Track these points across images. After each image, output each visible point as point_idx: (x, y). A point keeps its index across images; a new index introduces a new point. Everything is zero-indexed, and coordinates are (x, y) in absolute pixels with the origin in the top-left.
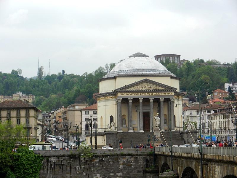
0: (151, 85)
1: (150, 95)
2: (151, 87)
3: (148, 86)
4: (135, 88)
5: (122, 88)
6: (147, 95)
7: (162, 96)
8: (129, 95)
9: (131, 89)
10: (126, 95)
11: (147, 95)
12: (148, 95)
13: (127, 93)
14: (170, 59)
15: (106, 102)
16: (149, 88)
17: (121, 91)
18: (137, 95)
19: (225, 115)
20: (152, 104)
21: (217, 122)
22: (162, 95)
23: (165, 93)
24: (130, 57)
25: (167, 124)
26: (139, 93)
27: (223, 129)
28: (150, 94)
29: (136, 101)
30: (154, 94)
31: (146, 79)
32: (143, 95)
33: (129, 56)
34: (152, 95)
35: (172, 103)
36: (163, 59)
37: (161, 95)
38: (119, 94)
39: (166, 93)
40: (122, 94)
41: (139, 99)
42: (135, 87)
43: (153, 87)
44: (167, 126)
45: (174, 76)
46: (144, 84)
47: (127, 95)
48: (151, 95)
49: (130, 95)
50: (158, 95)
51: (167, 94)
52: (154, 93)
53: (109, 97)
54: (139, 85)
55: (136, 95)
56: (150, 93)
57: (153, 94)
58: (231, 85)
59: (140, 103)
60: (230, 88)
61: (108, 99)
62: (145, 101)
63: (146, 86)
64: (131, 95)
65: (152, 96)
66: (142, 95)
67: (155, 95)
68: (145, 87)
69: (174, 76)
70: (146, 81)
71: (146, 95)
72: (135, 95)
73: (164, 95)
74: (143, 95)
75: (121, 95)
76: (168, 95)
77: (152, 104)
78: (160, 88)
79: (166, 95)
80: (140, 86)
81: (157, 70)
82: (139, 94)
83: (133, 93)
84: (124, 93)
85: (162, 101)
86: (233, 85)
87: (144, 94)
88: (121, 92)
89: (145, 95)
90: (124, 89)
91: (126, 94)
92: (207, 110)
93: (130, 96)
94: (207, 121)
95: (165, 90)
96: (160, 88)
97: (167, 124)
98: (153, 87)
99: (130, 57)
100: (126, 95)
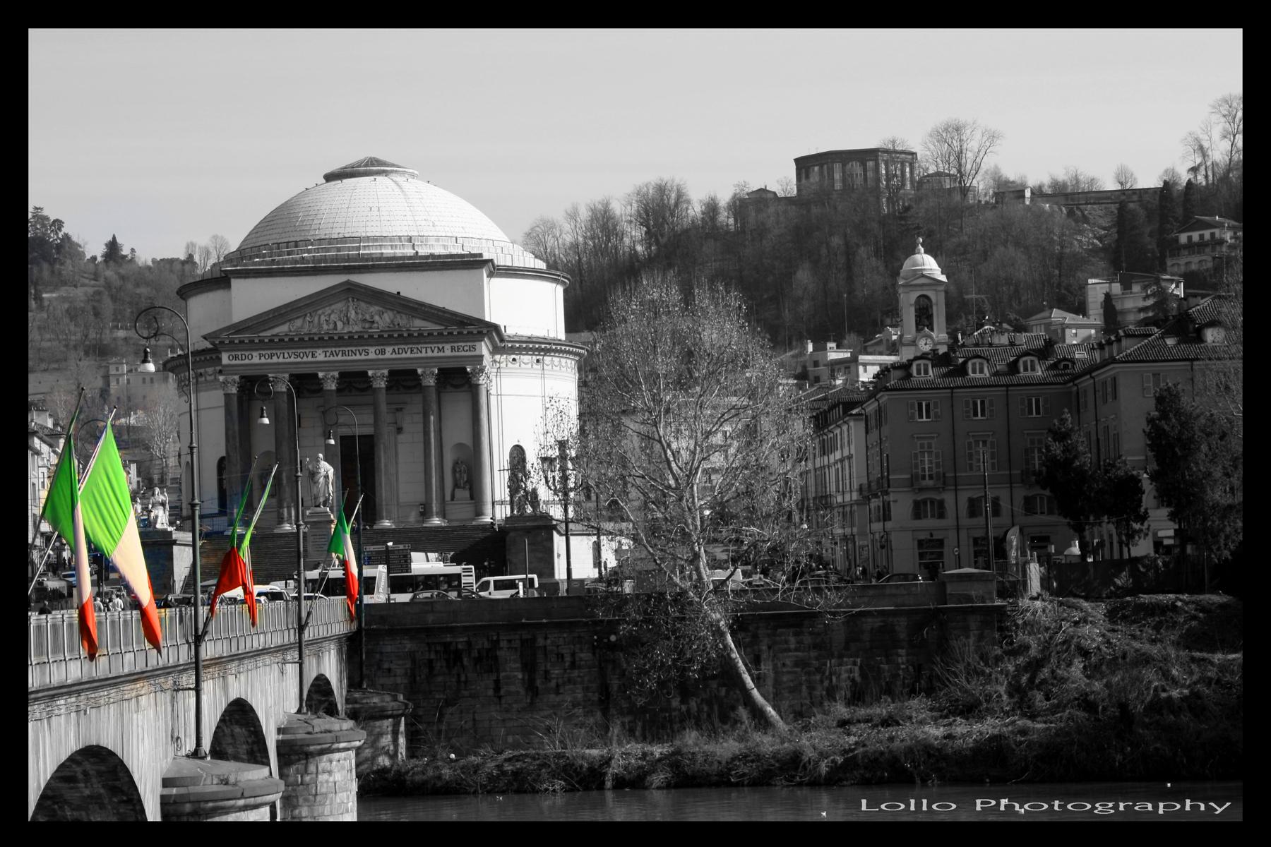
1: (372, 356)
2: (377, 318)
4: (297, 326)
5: (240, 328)
8: (269, 361)
9: (282, 329)
10: (256, 360)
11: (358, 357)
12: (363, 357)
14: (865, 171)
15: (202, 395)
16: (367, 325)
17: (231, 342)
18: (310, 359)
20: (382, 397)
22: (430, 354)
24: (330, 177)
26: (320, 351)
28: (372, 353)
29: (305, 383)
30: (389, 353)
31: (348, 282)
32: (340, 358)
33: (328, 171)
34: (380, 357)
37: (424, 355)
38: (225, 359)
39: (448, 347)
40: (236, 358)
42: (299, 323)
43: (384, 320)
45: (541, 265)
46: (340, 306)
47: (263, 360)
49: (275, 359)
50: (409, 355)
51: (453, 349)
52: (389, 349)
53: (210, 370)
55: (305, 359)
56: (372, 349)
57: (383, 352)
58: (1116, 288)
60: (1108, 297)
61: (209, 378)
63: (352, 315)
64: (281, 360)
65: (378, 360)
66: (332, 358)
67: (394, 356)
68: (331, 319)
69: (541, 265)
70: (352, 292)
71: (354, 358)
72: (299, 360)
73: (436, 354)
74: (336, 358)
75: (234, 362)
77: (382, 397)
79: (448, 353)
80: (323, 318)
81: (438, 238)
82: (320, 356)
86: (1126, 286)
88: (232, 346)
89: (345, 358)
90: (249, 333)
91: (255, 354)
93: (278, 363)
96: (419, 324)
97: (471, 489)
98: (384, 320)
99: (330, 177)
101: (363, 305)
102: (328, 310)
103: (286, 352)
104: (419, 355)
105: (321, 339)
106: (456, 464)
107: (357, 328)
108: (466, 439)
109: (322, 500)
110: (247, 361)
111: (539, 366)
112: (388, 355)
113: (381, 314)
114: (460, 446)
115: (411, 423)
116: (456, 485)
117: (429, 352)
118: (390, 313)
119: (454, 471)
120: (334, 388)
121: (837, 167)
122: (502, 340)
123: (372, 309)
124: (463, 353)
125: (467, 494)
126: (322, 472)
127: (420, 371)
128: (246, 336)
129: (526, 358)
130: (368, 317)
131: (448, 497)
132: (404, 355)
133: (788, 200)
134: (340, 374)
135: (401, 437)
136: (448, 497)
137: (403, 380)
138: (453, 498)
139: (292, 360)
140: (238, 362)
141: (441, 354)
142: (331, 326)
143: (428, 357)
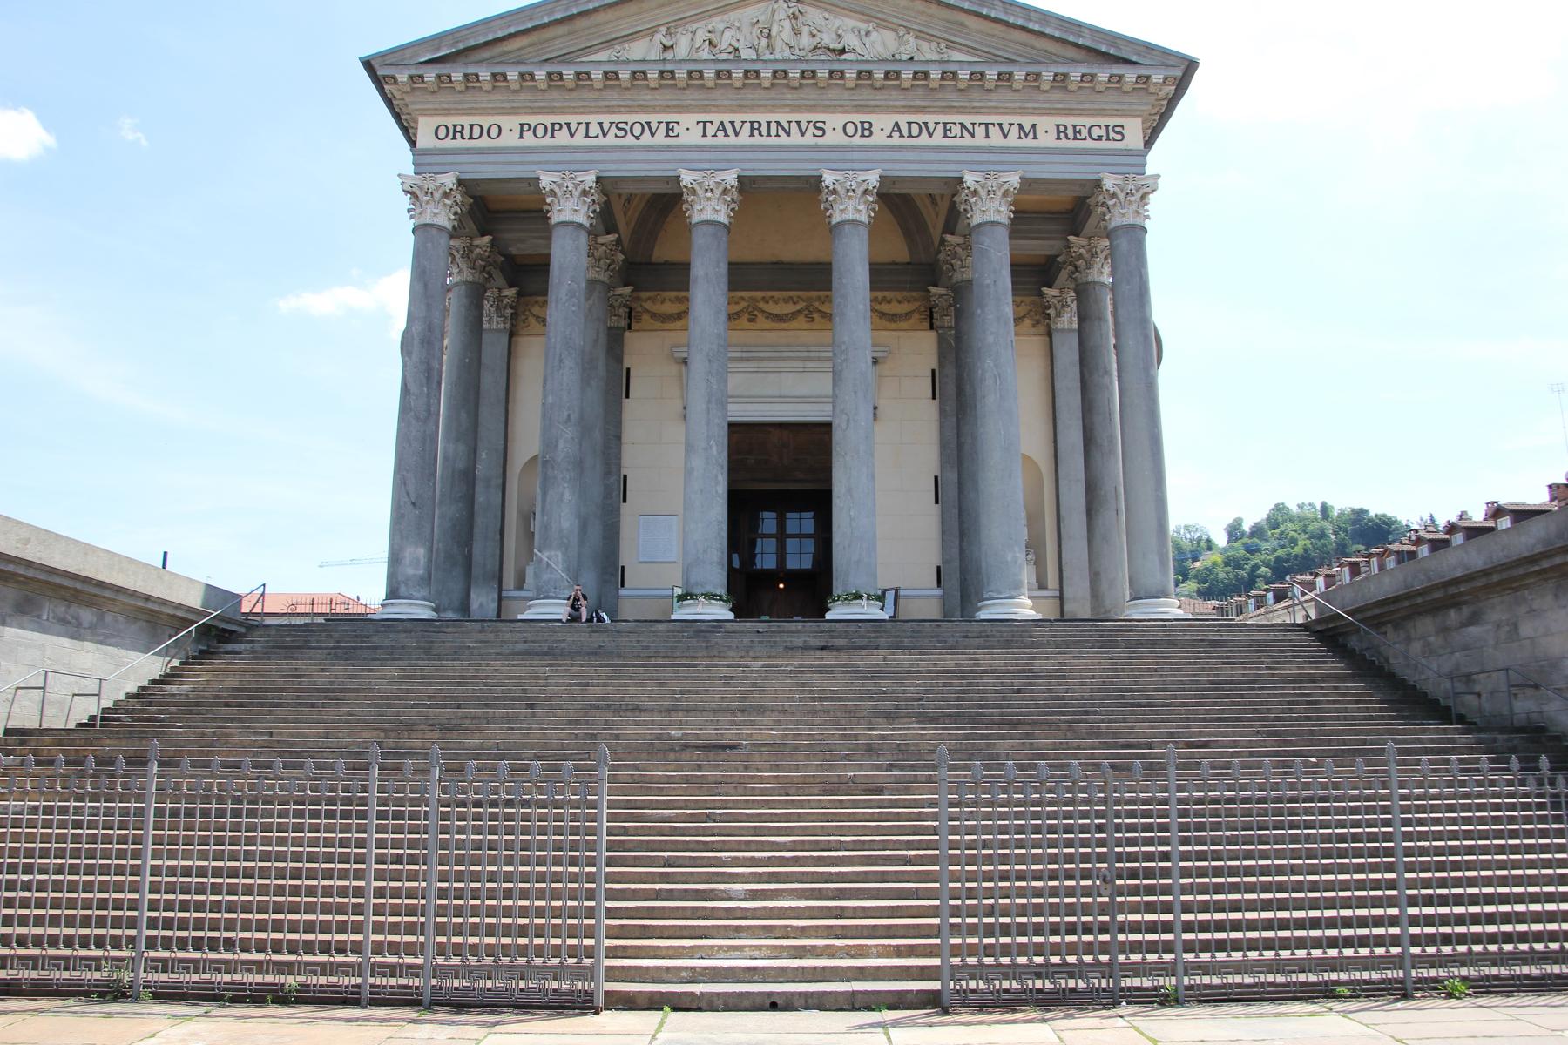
1: (834, 137)
2: (851, 40)
3: (805, 41)
6: (788, 139)
8: (547, 141)
10: (509, 139)
11: (796, 138)
12: (809, 139)
18: (660, 138)
22: (996, 139)
32: (744, 138)
34: (858, 140)
35: (1123, 243)
37: (980, 140)
39: (1046, 124)
40: (456, 131)
48: (845, 141)
49: (562, 138)
50: (938, 139)
51: (1060, 131)
52: (882, 123)
55: (646, 139)
56: (834, 121)
57: (866, 129)
59: (700, 239)
62: (789, 308)
64: (579, 140)
66: (721, 139)
67: (896, 140)
71: (783, 139)
73: (1013, 140)
74: (732, 140)
75: (449, 143)
79: (1047, 139)
82: (689, 129)
83: (606, 119)
84: (485, 122)
87: (755, 128)
89: (757, 140)
91: (510, 123)
100: (508, 140)
101: (814, 15)
102: (717, 23)
103: (594, 119)
104: (968, 141)
110: (485, 142)
112: (879, 138)
118: (889, 36)
123: (838, 23)
124: (1089, 144)
130: (828, 39)
132: (924, 140)
139: (610, 140)
140: (459, 143)
141: (1028, 142)
143: (994, 154)
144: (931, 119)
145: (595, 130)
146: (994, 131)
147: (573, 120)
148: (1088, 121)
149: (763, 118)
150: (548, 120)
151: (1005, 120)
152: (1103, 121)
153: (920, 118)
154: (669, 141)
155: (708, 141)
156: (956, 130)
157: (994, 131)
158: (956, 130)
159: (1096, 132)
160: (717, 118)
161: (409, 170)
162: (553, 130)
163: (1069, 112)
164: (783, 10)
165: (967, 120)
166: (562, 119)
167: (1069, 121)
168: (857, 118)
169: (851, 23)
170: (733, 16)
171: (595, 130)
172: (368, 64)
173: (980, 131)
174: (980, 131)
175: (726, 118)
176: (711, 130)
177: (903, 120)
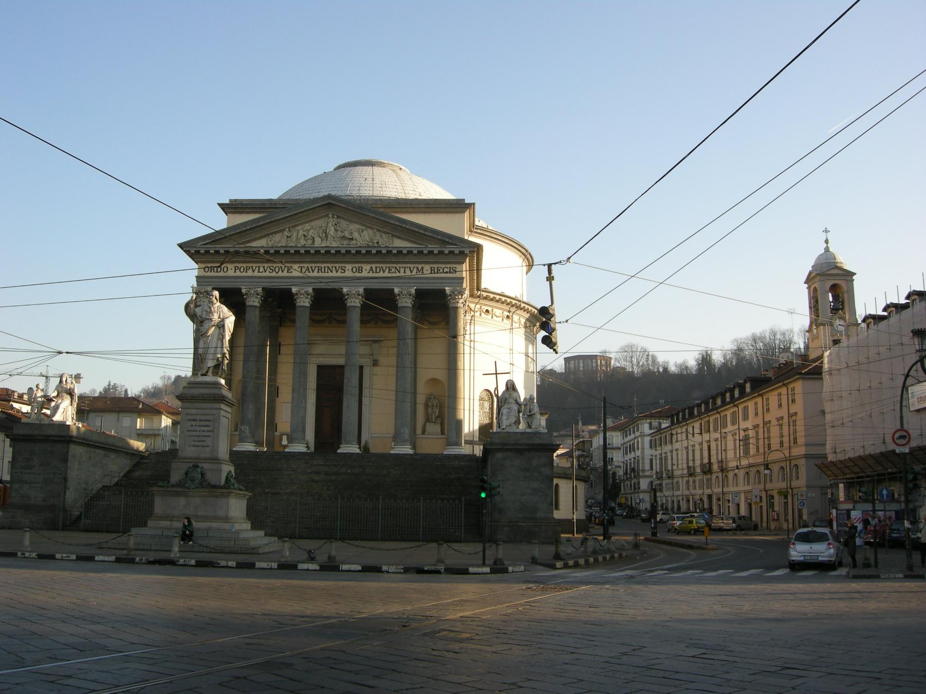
0: (354, 227)
1: (349, 274)
2: (356, 235)
3: (339, 234)
7: (405, 279)
8: (244, 274)
10: (231, 273)
11: (334, 274)
12: (339, 274)
13: (239, 265)
16: (345, 242)
17: (207, 252)
18: (285, 274)
19: (709, 421)
21: (677, 450)
22: (408, 273)
23: (420, 267)
24: (335, 169)
25: (442, 424)
26: (296, 266)
27: (698, 470)
28: (349, 271)
29: (279, 302)
30: (366, 270)
32: (315, 274)
34: (357, 275)
36: (579, 363)
37: (402, 274)
41: (294, 290)
42: (277, 237)
43: (363, 237)
44: (443, 433)
46: (320, 223)
47: (238, 273)
49: (250, 273)
50: (386, 274)
51: (432, 271)
52: (366, 267)
54: (299, 227)
55: (280, 274)
57: (360, 270)
59: (298, 311)
64: (256, 274)
65: (353, 279)
67: (371, 275)
71: (330, 274)
72: (274, 274)
75: (209, 274)
76: (436, 275)
77: (355, 318)
78: (399, 243)
80: (301, 233)
82: (296, 271)
83: (266, 265)
85: (406, 302)
87: (320, 270)
89: (320, 274)
92: (648, 421)
94: (648, 452)
95: (420, 252)
96: (399, 243)
97: (442, 424)
98: (363, 237)
101: (343, 223)
102: (307, 226)
104: (397, 274)
105: (297, 252)
106: (428, 399)
107: (334, 244)
108: (441, 375)
109: (211, 364)
111: (508, 322)
112: (365, 274)
113: (360, 232)
114: (434, 381)
115: (388, 359)
116: (428, 420)
117: (406, 271)
118: (370, 231)
119: (426, 406)
120: (307, 304)
121: (581, 361)
122: (478, 289)
125: (437, 428)
126: (215, 317)
127: (396, 290)
128: (221, 248)
129: (498, 312)
130: (347, 235)
131: (419, 431)
132: (381, 274)
133: (561, 373)
134: (314, 289)
135: (376, 369)
136: (419, 431)
137: (380, 303)
138: (424, 432)
139: (267, 274)
142: (310, 242)
144: (384, 266)
145: (262, 269)
146: (408, 271)
147: (254, 265)
148: (443, 266)
149: (323, 265)
150: (245, 265)
151: (412, 266)
152: (449, 266)
153: (380, 265)
154: (288, 275)
155: (301, 275)
156: (393, 270)
157: (408, 271)
158: (393, 270)
159: (446, 270)
160: (306, 265)
161: (195, 285)
162: (246, 270)
163: (436, 263)
164: (332, 222)
165: (397, 266)
166: (250, 265)
167: (435, 266)
168: (357, 265)
169: (357, 226)
170: (313, 224)
171: (262, 269)
172: (181, 246)
173: (402, 270)
174: (402, 270)
175: (309, 265)
176: (304, 270)
177: (374, 266)
